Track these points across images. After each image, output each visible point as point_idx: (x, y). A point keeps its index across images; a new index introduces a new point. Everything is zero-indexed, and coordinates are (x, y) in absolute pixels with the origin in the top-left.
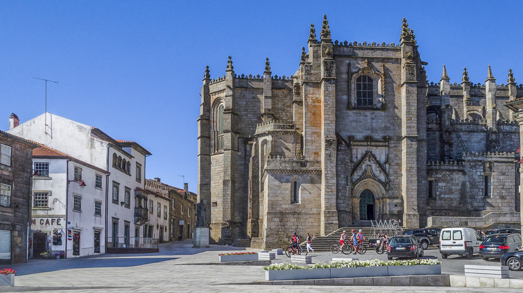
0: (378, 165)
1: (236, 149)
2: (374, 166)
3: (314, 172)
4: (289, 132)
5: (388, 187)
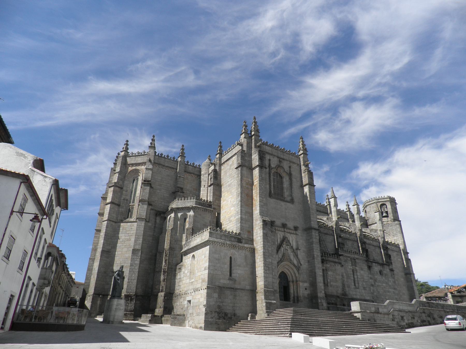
0: (292, 250)
1: (147, 220)
2: (290, 251)
3: (248, 249)
4: (208, 210)
5: (300, 272)
